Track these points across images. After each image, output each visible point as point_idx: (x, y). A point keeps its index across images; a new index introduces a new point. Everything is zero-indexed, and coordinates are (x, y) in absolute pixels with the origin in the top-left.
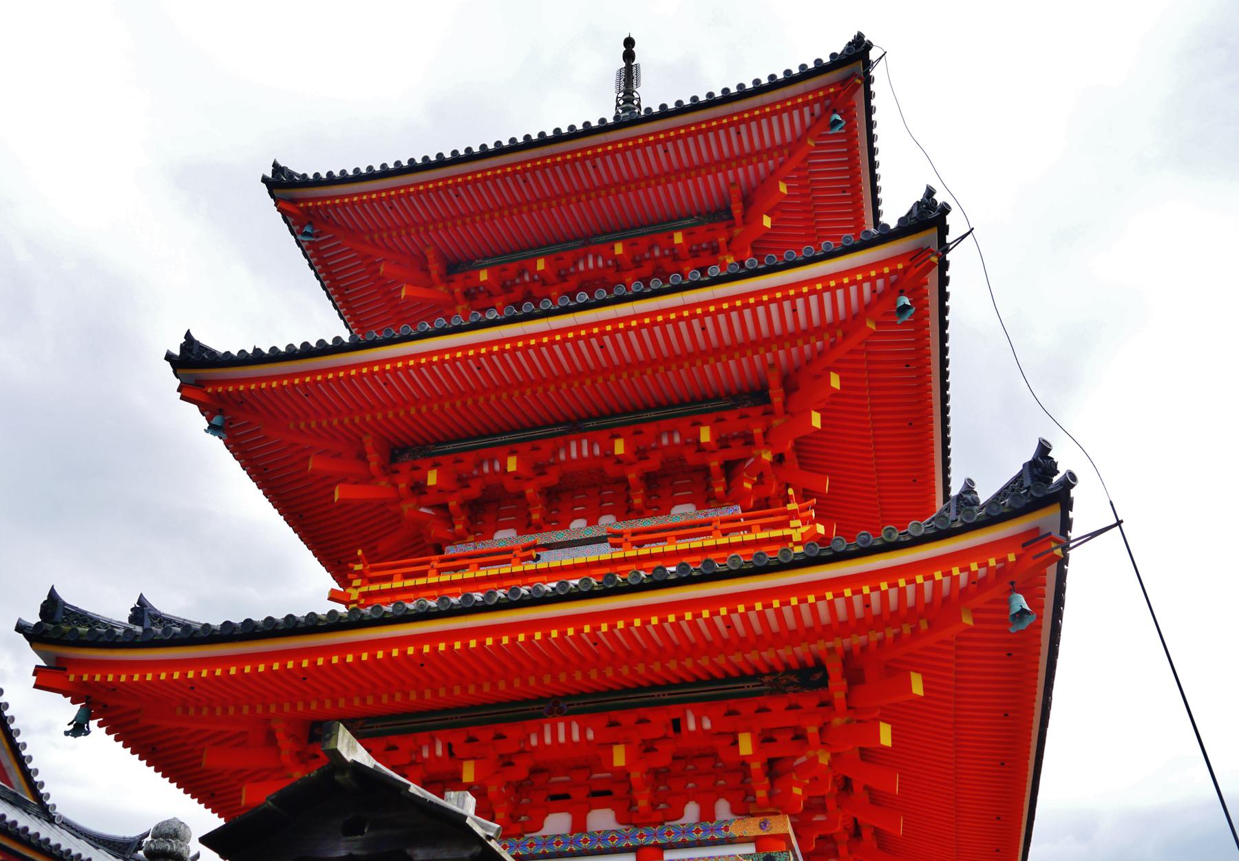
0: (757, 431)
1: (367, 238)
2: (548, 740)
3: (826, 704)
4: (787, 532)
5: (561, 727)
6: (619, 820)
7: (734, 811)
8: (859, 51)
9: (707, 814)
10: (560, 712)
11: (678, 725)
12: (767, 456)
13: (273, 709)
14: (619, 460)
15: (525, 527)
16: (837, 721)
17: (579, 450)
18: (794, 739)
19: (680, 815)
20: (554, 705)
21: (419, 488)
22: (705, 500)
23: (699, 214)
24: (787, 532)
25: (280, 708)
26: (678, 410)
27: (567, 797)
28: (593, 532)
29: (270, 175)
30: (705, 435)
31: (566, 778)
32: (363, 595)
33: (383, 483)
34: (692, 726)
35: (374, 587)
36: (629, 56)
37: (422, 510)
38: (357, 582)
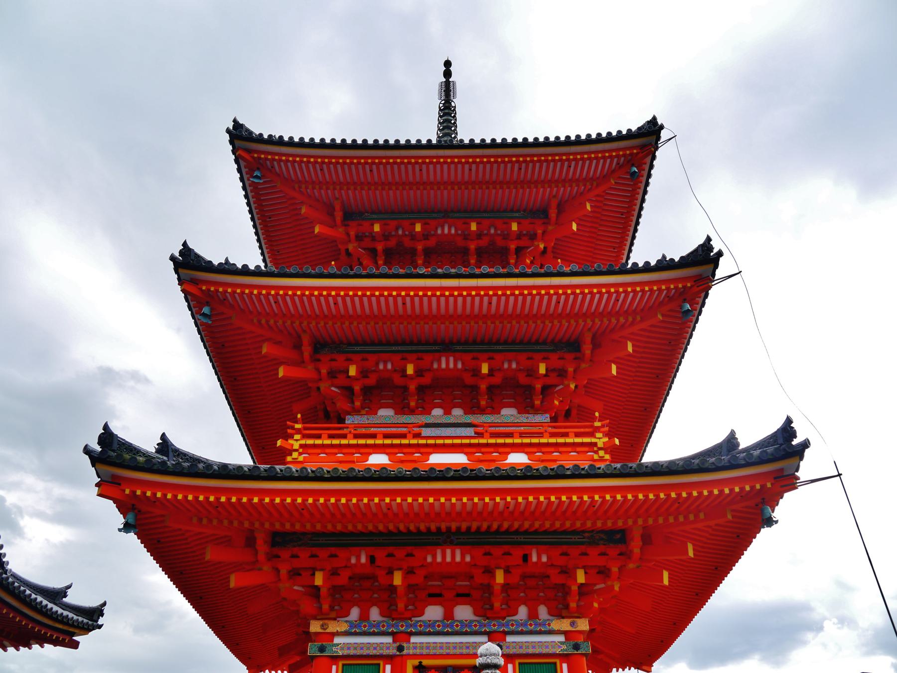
0: (571, 369)
1: (296, 186)
4: (594, 440)
5: (448, 552)
6: (476, 614)
7: (550, 614)
9: (533, 615)
10: (451, 542)
11: (526, 558)
13: (257, 525)
15: (402, 408)
17: (447, 363)
18: (598, 573)
19: (516, 613)
20: (446, 538)
23: (524, 211)
25: (262, 525)
26: (517, 347)
27: (440, 595)
31: (440, 583)
32: (301, 446)
33: (310, 367)
35: (310, 442)
36: (447, 74)
37: (333, 389)
38: (297, 437)
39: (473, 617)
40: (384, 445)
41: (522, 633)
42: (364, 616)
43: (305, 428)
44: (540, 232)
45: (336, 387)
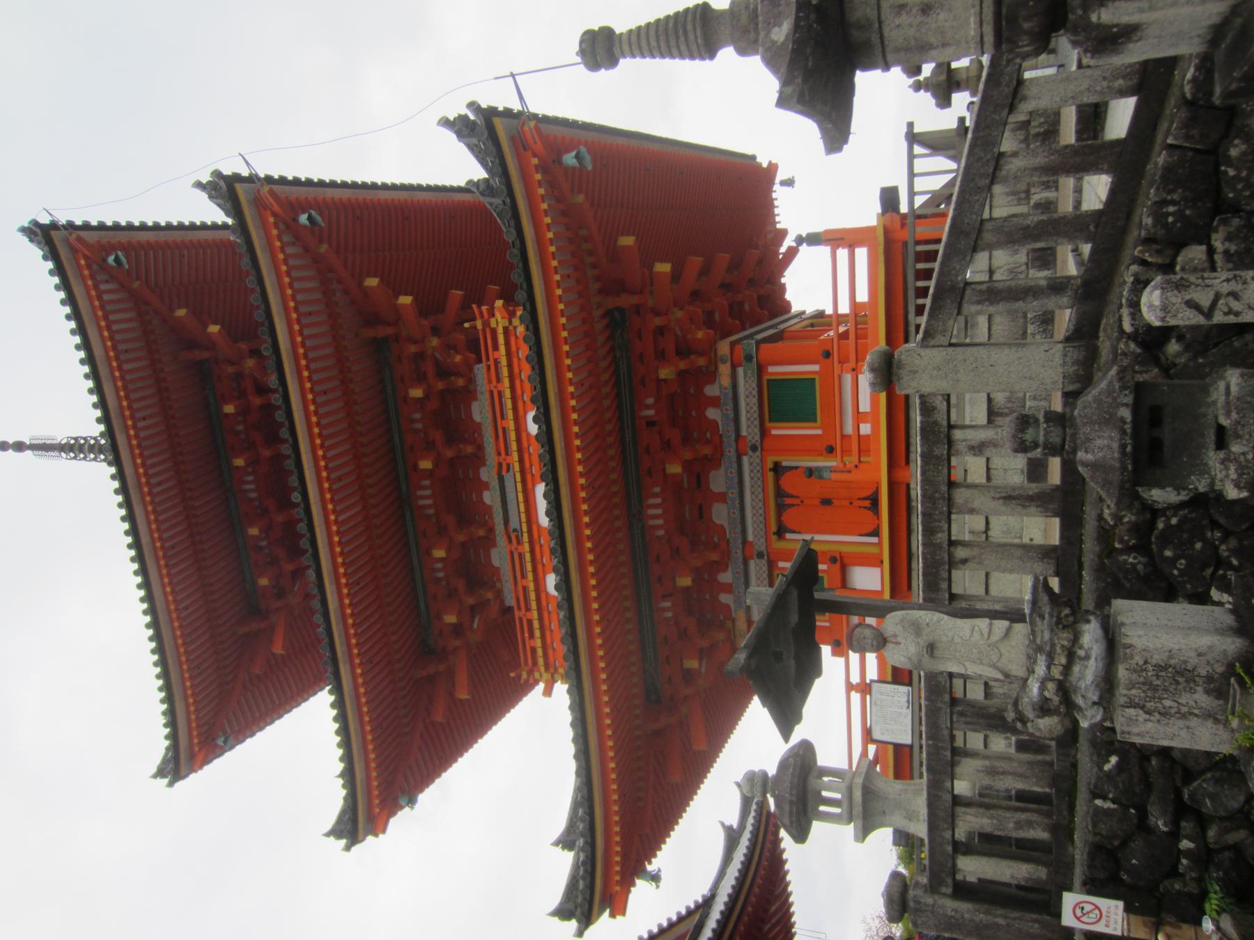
2: (660, 522)
3: (637, 309)
4: (500, 330)
6: (718, 466)
8: (46, 235)
9: (715, 402)
11: (650, 423)
12: (435, 342)
14: (436, 465)
15: (489, 541)
16: (651, 303)
17: (425, 497)
21: (457, 630)
22: (469, 394)
24: (500, 330)
27: (700, 507)
28: (495, 483)
29: (166, 781)
30: (417, 393)
32: (547, 669)
34: (651, 412)
35: (541, 661)
37: (475, 626)
39: (722, 470)
40: (536, 580)
41: (737, 420)
42: (728, 588)
43: (526, 663)
44: (230, 370)
45: (473, 621)
